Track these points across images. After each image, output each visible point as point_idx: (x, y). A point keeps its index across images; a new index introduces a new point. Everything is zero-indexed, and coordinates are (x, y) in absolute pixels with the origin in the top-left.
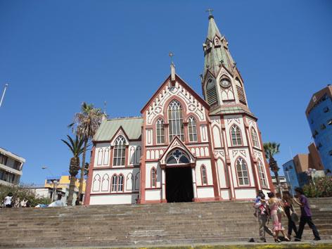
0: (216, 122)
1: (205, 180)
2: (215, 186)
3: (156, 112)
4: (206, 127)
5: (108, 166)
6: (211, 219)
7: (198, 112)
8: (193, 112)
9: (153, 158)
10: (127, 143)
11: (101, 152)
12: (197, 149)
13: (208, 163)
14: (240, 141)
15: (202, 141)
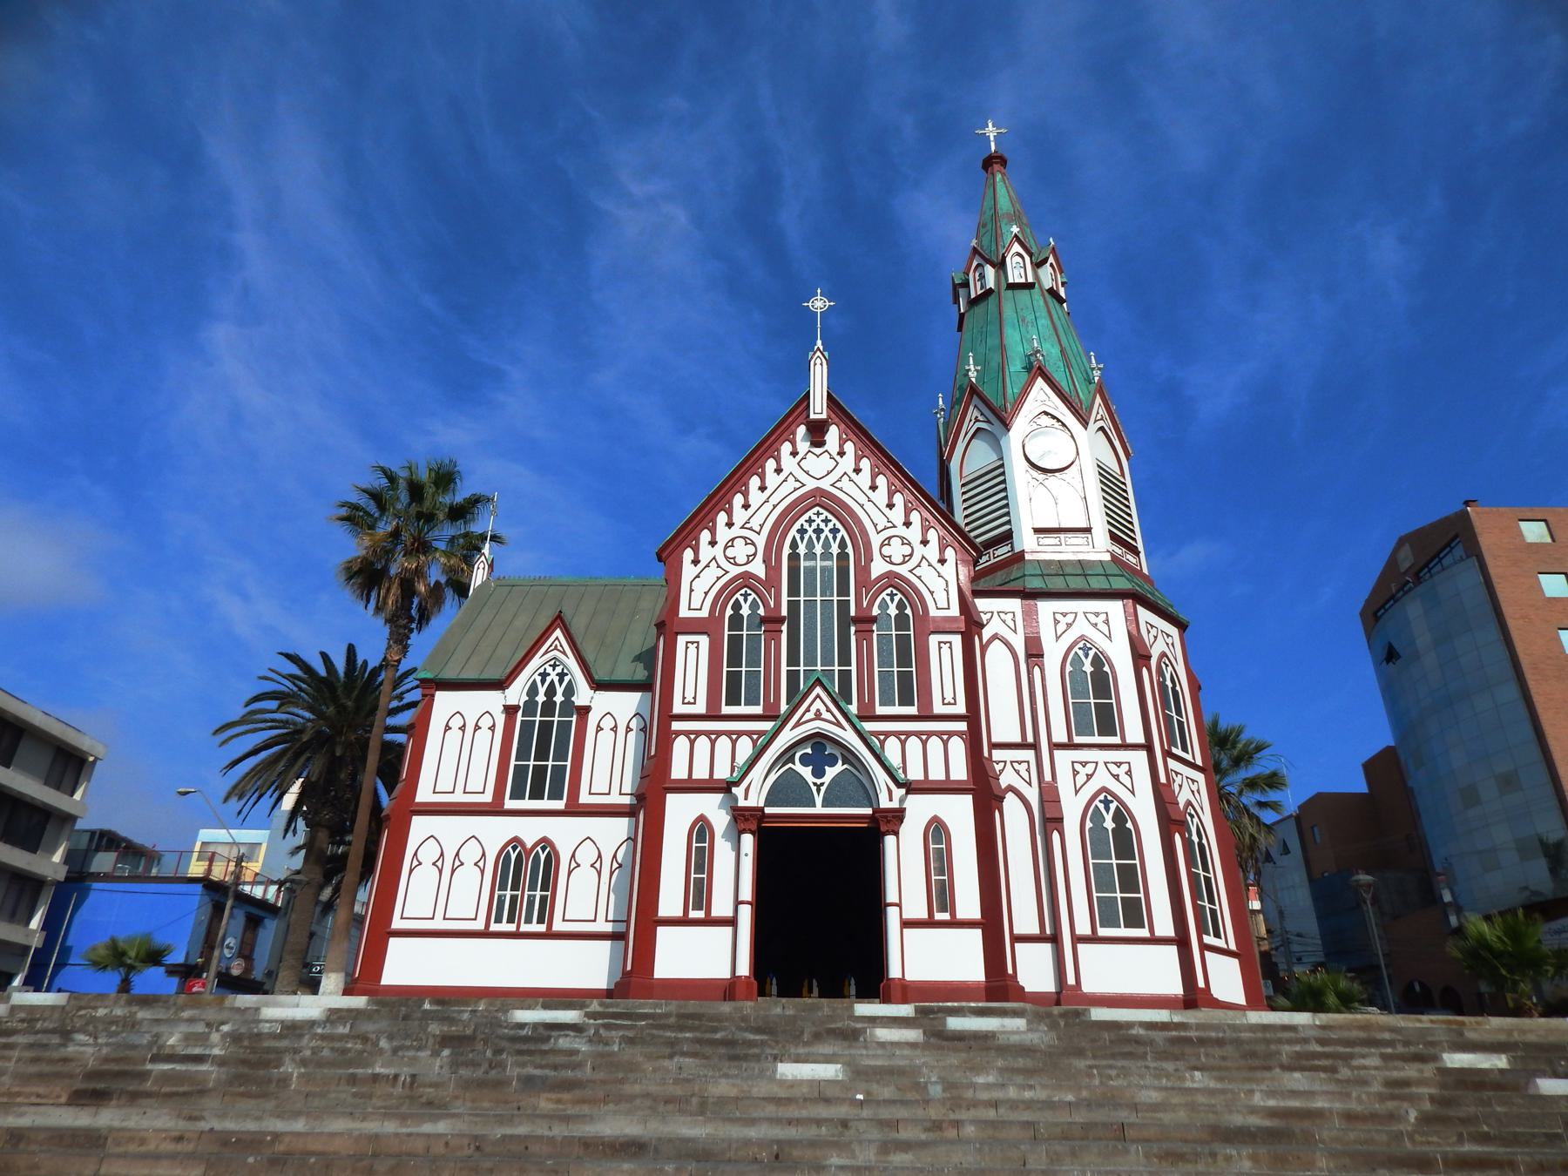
0: (999, 613)
1: (942, 895)
2: (992, 923)
4: (957, 640)
5: (488, 798)
6: (995, 1104)
7: (924, 571)
8: (903, 570)
9: (701, 773)
10: (583, 695)
11: (455, 734)
12: (914, 744)
13: (959, 813)
15: (938, 709)
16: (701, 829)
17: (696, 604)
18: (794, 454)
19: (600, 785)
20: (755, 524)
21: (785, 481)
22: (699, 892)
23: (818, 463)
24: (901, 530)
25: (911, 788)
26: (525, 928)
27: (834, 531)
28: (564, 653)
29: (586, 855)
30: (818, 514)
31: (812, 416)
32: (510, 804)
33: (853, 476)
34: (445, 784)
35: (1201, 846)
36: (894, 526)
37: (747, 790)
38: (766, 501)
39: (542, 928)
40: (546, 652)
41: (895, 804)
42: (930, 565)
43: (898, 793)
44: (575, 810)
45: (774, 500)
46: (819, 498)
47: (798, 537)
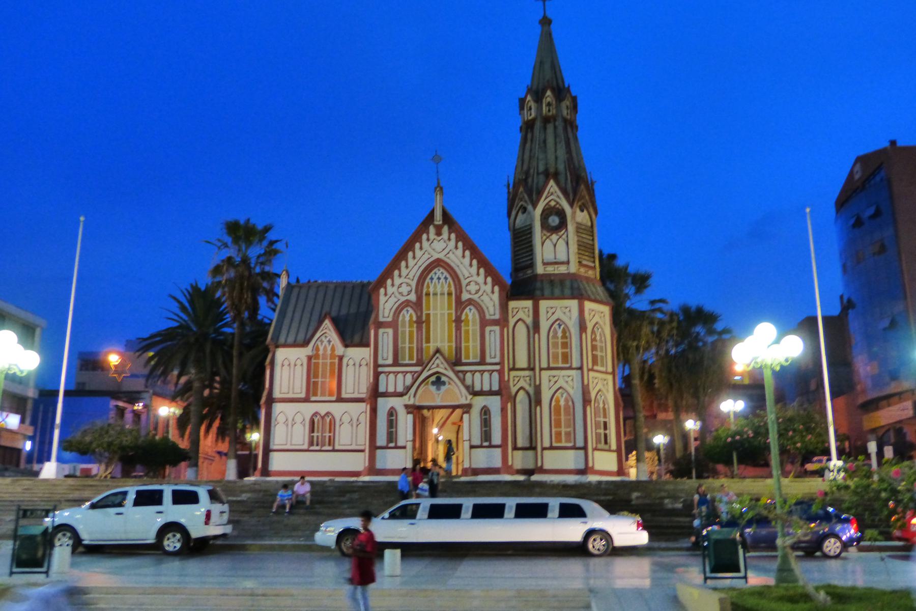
0: (521, 308)
1: (486, 435)
3: (401, 293)
8: (475, 297)
11: (286, 367)
12: (477, 375)
14: (566, 358)
16: (392, 413)
17: (386, 315)
18: (428, 240)
19: (350, 390)
20: (411, 276)
21: (424, 254)
22: (392, 436)
23: (439, 245)
24: (475, 278)
25: (476, 394)
26: (324, 448)
27: (446, 278)
28: (330, 330)
29: (346, 419)
30: (439, 270)
31: (436, 223)
32: (313, 399)
33: (454, 250)
34: (285, 390)
35: (604, 409)
36: (472, 276)
37: (410, 397)
38: (416, 264)
39: (330, 448)
40: (322, 330)
41: (468, 402)
42: (487, 295)
43: (470, 397)
44: (340, 400)
45: (420, 263)
46: (438, 263)
47: (430, 281)
